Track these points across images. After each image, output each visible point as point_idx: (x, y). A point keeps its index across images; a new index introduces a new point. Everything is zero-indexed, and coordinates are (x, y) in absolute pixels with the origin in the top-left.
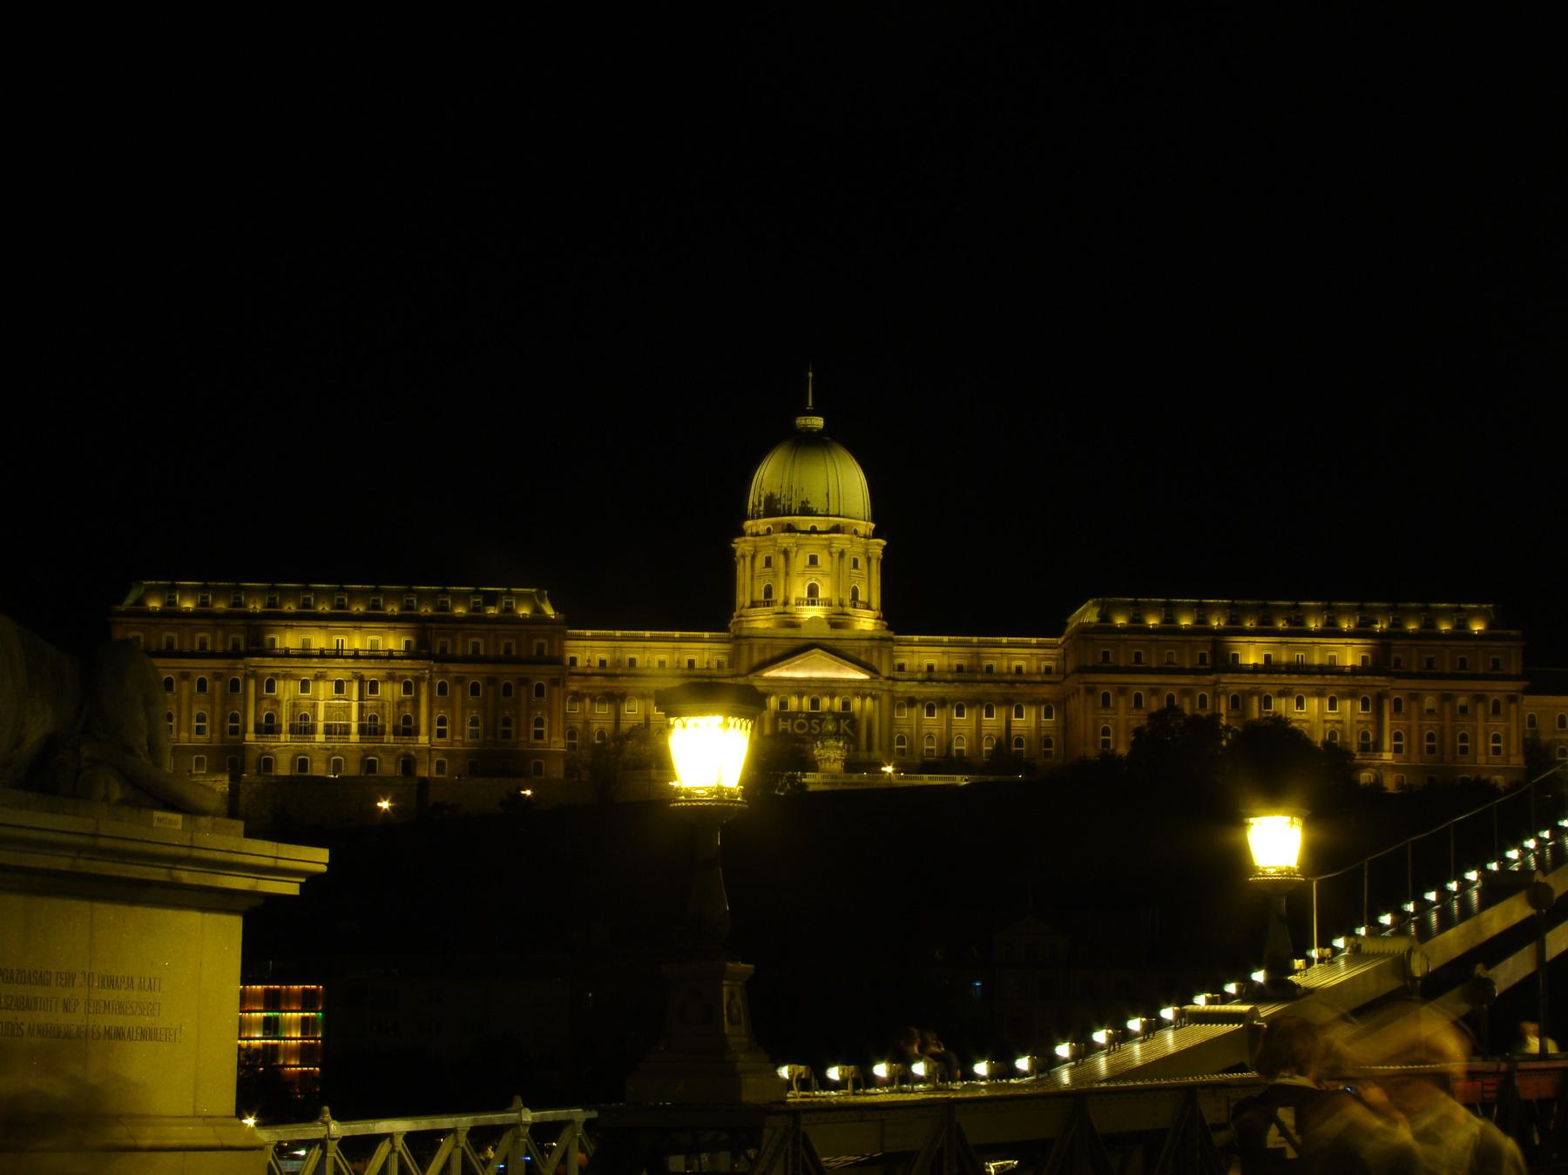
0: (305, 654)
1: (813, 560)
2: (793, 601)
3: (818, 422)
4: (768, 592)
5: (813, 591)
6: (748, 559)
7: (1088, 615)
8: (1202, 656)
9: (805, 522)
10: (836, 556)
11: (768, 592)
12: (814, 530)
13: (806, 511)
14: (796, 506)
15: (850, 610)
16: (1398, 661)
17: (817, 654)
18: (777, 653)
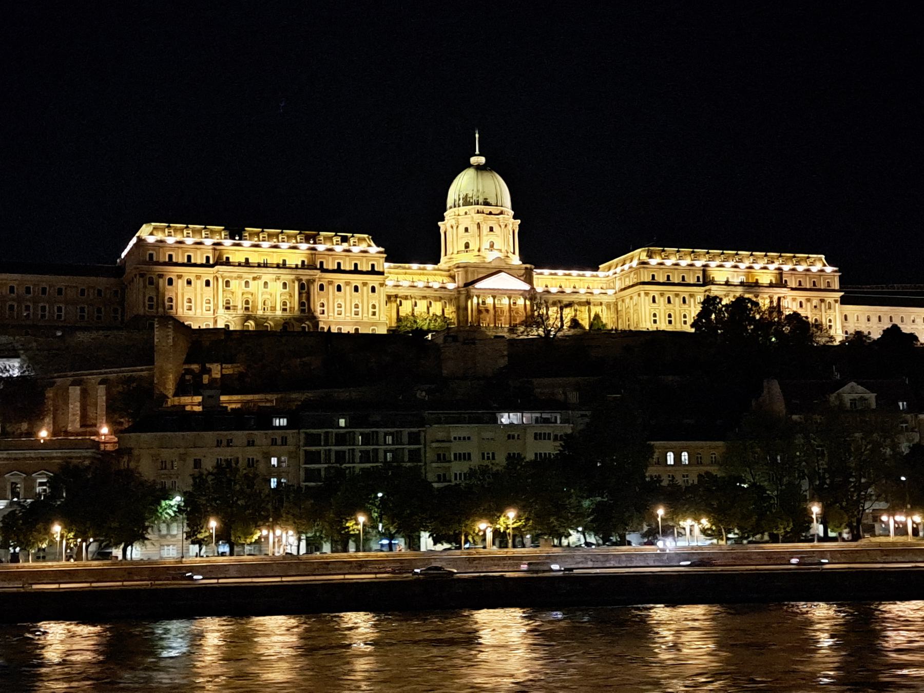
0: (247, 264)
1: (491, 229)
2: (483, 249)
3: (482, 160)
4: (467, 246)
5: (492, 245)
6: (455, 228)
7: (640, 254)
8: (698, 278)
9: (487, 209)
10: (503, 227)
11: (467, 246)
12: (490, 213)
13: (486, 203)
14: (481, 201)
15: (510, 255)
16: (786, 281)
17: (502, 274)
18: (481, 276)
